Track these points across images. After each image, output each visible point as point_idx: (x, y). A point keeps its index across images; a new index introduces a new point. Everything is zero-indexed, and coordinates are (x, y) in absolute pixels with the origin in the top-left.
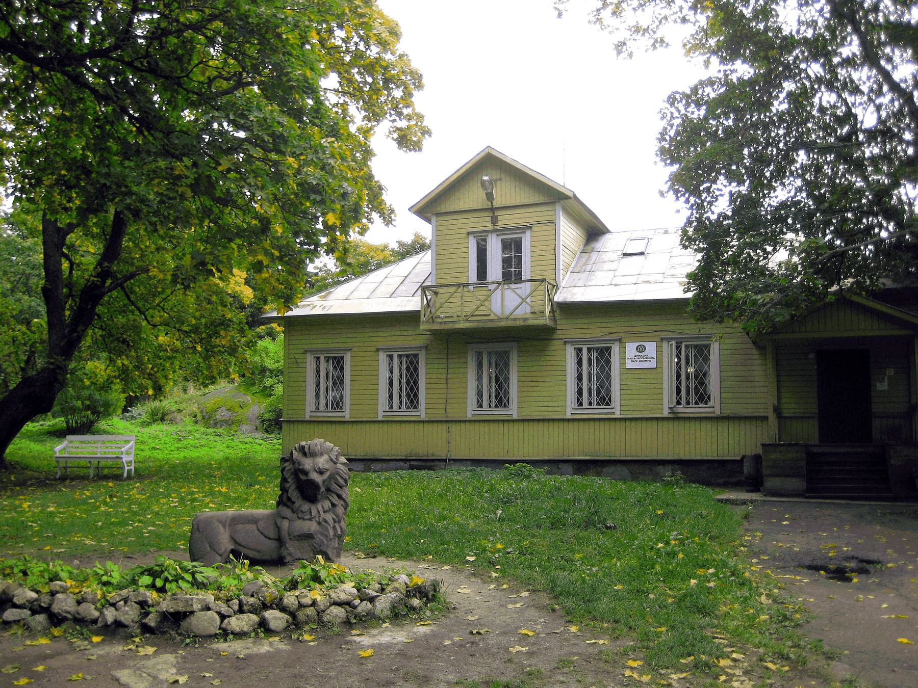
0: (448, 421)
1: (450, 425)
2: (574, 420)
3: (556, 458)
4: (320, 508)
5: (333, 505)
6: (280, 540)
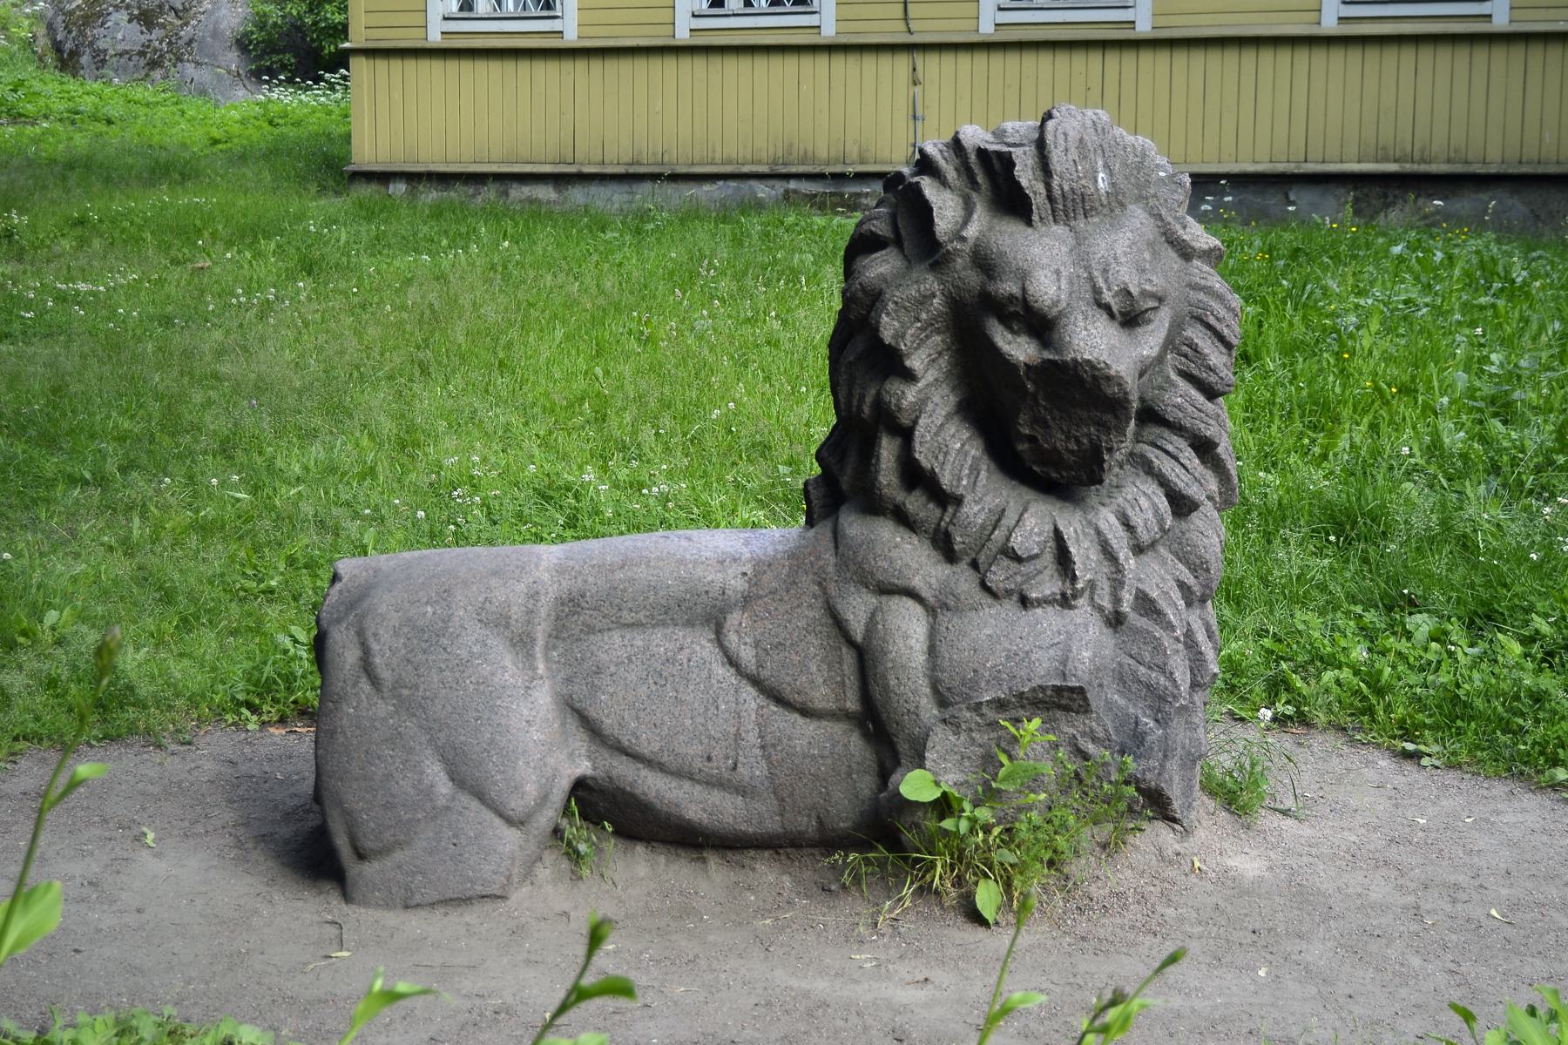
1: (919, 58)
3: (1281, 167)
4: (1108, 520)
5: (1181, 505)
6: (884, 736)
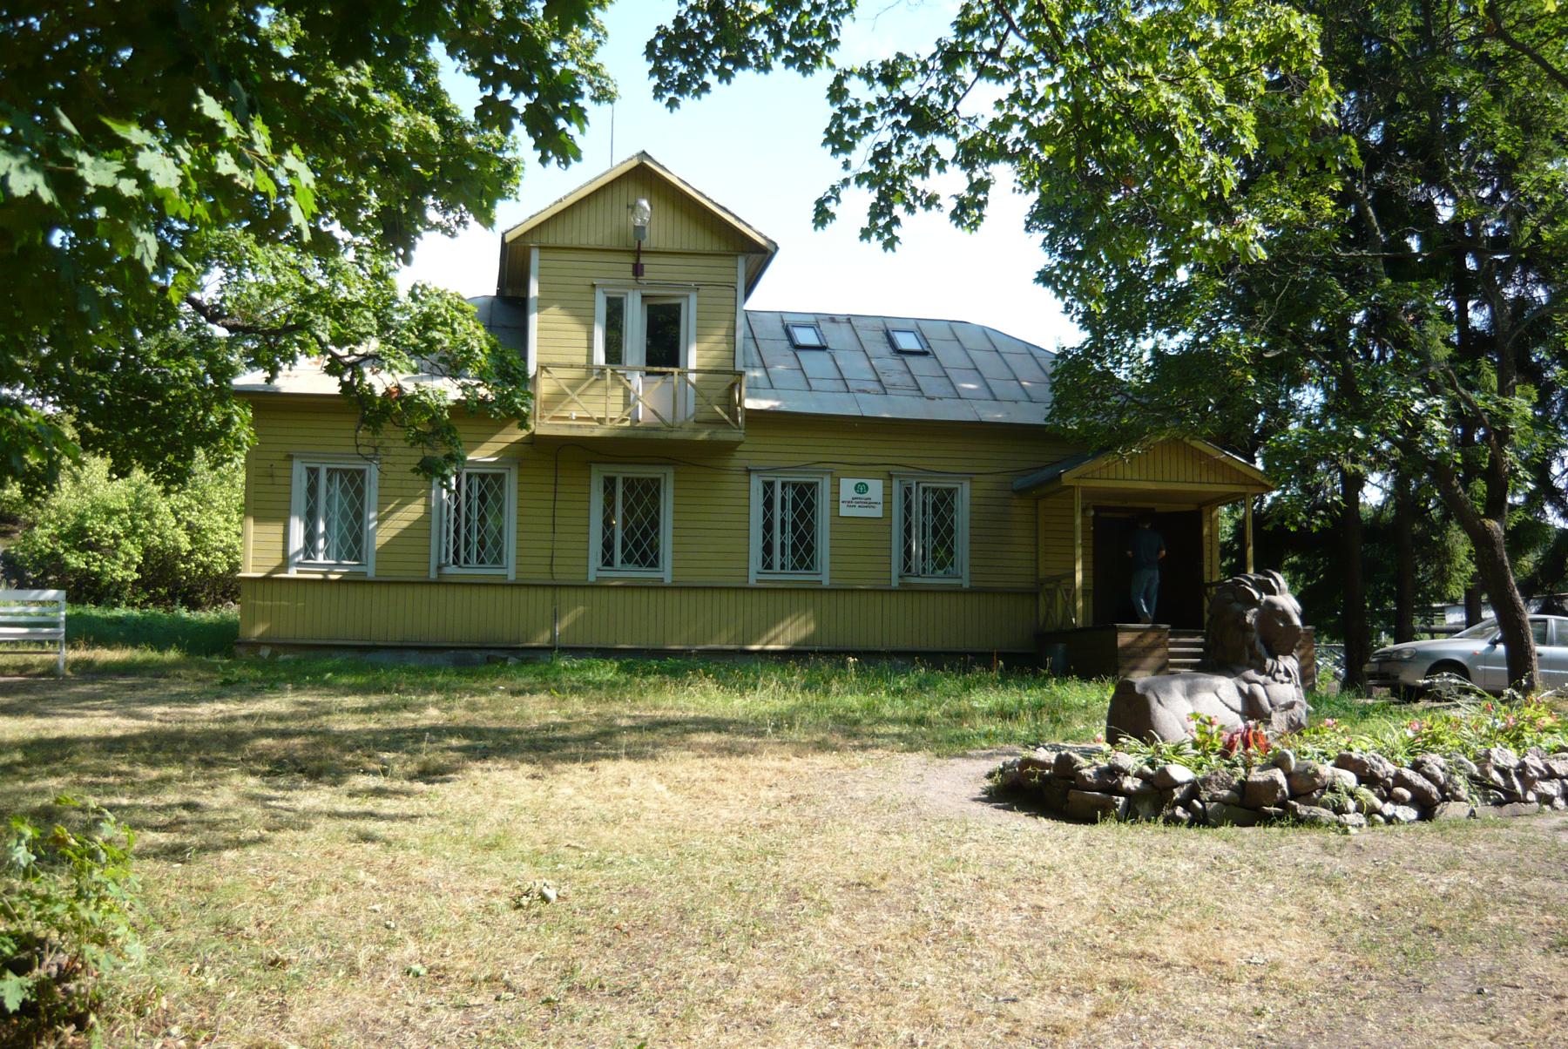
0: (554, 587)
2: (760, 589)
